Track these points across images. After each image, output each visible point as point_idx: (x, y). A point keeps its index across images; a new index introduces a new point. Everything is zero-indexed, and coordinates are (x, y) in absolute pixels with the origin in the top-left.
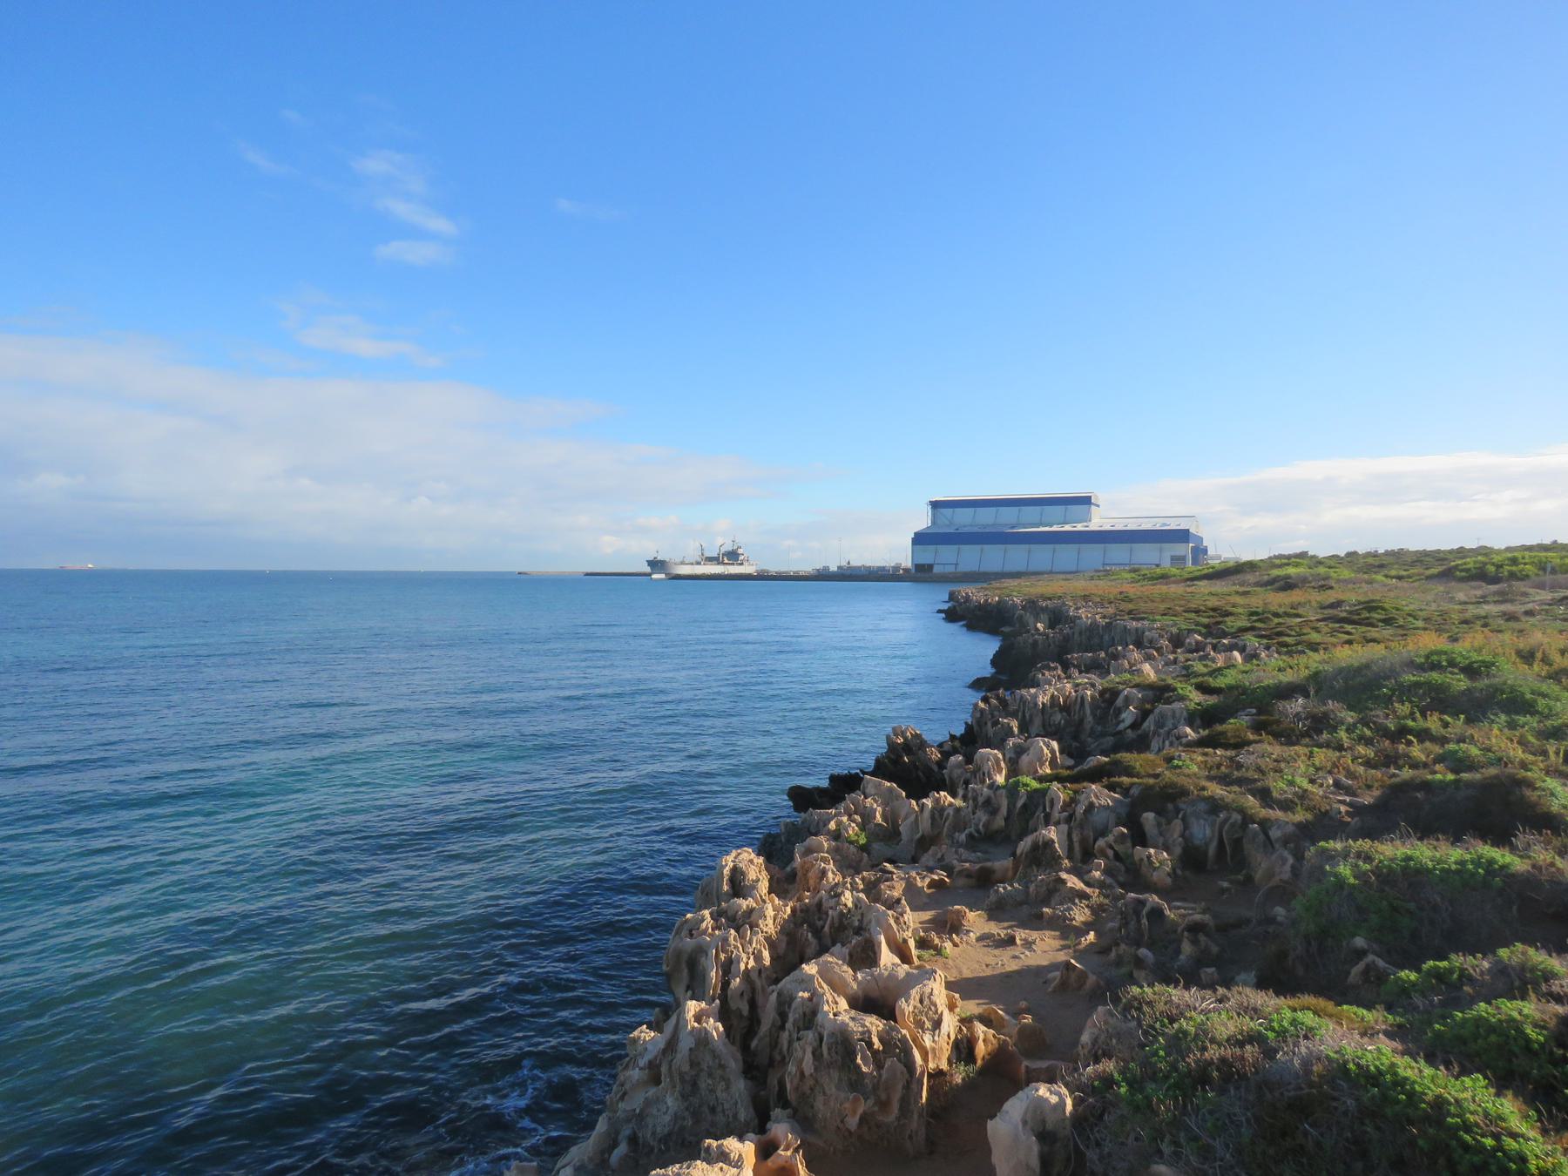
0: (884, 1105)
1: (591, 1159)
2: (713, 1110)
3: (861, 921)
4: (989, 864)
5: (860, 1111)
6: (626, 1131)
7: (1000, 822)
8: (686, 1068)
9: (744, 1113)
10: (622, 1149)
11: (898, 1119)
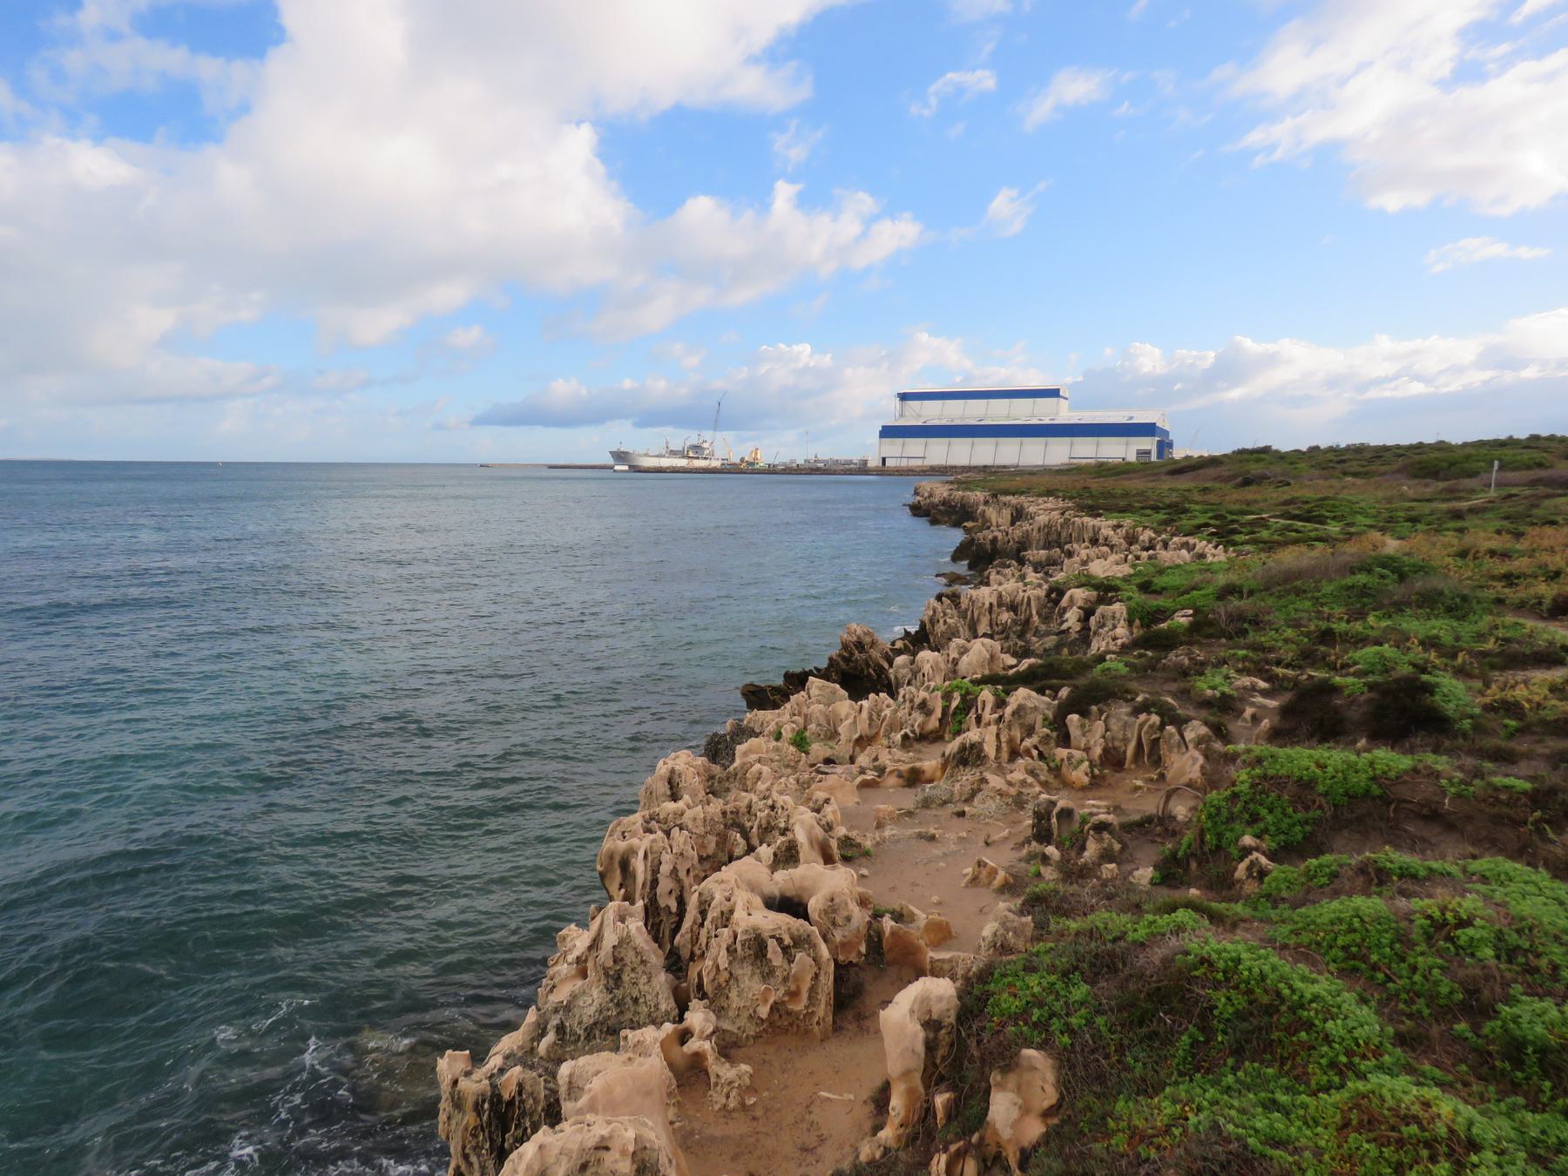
0: (794, 995)
1: (521, 1048)
2: (636, 1001)
3: (787, 822)
4: (918, 764)
5: (771, 1001)
6: (555, 1021)
7: (933, 723)
8: (610, 963)
9: (667, 1004)
10: (550, 1037)
11: (807, 1007)
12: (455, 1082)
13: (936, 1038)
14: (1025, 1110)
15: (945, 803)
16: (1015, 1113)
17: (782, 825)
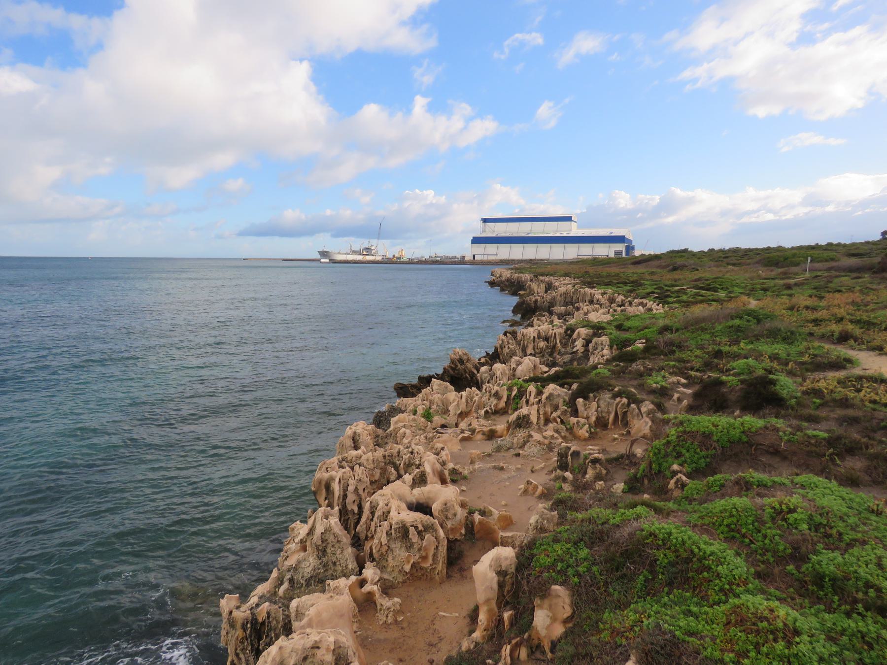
0: (424, 558)
1: (269, 592)
2: (334, 564)
3: (420, 461)
4: (494, 427)
6: (288, 576)
7: (502, 404)
9: (352, 565)
10: (286, 585)
11: (432, 565)
12: (231, 612)
13: (504, 580)
14: (554, 619)
15: (509, 449)
16: (548, 621)
17: (417, 463)
